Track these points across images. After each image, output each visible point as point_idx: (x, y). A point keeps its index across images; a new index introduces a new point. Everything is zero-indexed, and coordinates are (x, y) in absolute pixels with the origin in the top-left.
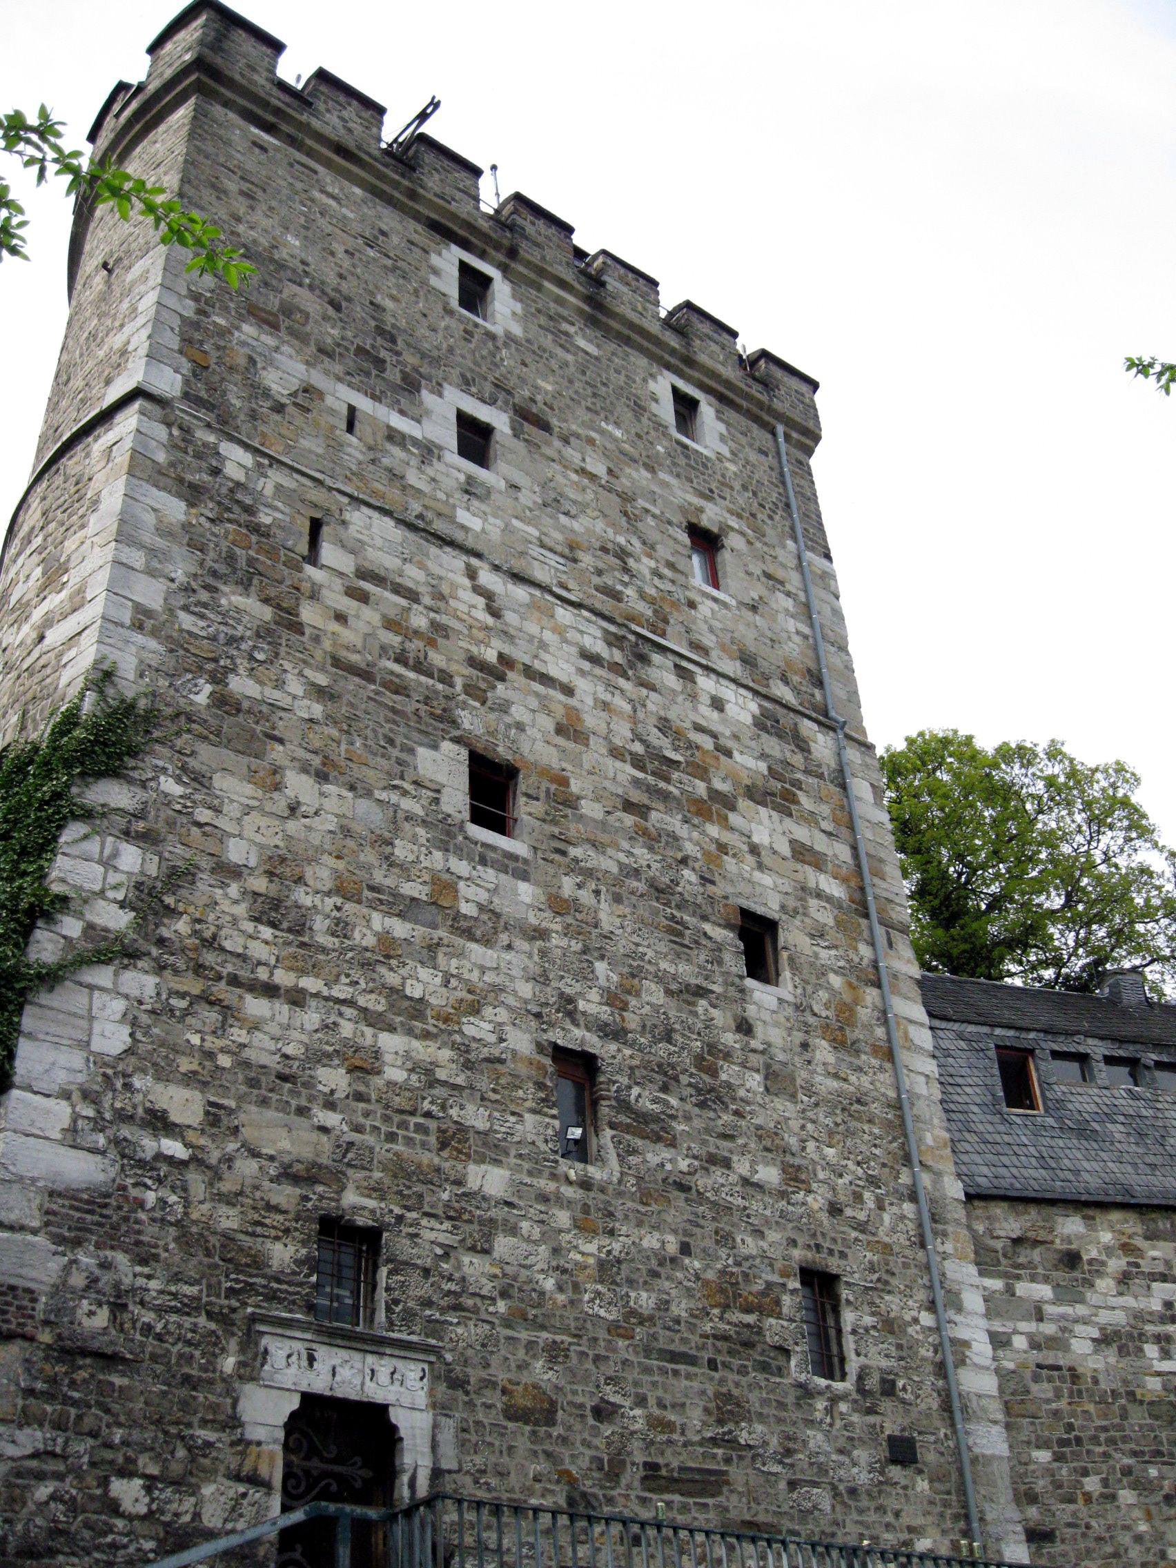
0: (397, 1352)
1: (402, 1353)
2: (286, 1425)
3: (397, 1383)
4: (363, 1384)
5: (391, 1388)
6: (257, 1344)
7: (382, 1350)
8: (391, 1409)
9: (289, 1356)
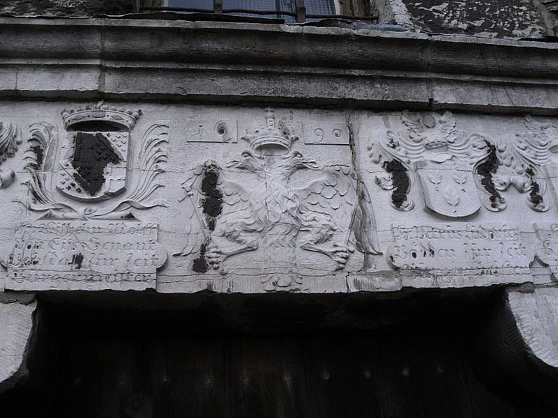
0: (480, 97)
1: (502, 99)
3: (517, 202)
4: (361, 224)
5: (490, 220)
7: (418, 94)
8: (514, 300)
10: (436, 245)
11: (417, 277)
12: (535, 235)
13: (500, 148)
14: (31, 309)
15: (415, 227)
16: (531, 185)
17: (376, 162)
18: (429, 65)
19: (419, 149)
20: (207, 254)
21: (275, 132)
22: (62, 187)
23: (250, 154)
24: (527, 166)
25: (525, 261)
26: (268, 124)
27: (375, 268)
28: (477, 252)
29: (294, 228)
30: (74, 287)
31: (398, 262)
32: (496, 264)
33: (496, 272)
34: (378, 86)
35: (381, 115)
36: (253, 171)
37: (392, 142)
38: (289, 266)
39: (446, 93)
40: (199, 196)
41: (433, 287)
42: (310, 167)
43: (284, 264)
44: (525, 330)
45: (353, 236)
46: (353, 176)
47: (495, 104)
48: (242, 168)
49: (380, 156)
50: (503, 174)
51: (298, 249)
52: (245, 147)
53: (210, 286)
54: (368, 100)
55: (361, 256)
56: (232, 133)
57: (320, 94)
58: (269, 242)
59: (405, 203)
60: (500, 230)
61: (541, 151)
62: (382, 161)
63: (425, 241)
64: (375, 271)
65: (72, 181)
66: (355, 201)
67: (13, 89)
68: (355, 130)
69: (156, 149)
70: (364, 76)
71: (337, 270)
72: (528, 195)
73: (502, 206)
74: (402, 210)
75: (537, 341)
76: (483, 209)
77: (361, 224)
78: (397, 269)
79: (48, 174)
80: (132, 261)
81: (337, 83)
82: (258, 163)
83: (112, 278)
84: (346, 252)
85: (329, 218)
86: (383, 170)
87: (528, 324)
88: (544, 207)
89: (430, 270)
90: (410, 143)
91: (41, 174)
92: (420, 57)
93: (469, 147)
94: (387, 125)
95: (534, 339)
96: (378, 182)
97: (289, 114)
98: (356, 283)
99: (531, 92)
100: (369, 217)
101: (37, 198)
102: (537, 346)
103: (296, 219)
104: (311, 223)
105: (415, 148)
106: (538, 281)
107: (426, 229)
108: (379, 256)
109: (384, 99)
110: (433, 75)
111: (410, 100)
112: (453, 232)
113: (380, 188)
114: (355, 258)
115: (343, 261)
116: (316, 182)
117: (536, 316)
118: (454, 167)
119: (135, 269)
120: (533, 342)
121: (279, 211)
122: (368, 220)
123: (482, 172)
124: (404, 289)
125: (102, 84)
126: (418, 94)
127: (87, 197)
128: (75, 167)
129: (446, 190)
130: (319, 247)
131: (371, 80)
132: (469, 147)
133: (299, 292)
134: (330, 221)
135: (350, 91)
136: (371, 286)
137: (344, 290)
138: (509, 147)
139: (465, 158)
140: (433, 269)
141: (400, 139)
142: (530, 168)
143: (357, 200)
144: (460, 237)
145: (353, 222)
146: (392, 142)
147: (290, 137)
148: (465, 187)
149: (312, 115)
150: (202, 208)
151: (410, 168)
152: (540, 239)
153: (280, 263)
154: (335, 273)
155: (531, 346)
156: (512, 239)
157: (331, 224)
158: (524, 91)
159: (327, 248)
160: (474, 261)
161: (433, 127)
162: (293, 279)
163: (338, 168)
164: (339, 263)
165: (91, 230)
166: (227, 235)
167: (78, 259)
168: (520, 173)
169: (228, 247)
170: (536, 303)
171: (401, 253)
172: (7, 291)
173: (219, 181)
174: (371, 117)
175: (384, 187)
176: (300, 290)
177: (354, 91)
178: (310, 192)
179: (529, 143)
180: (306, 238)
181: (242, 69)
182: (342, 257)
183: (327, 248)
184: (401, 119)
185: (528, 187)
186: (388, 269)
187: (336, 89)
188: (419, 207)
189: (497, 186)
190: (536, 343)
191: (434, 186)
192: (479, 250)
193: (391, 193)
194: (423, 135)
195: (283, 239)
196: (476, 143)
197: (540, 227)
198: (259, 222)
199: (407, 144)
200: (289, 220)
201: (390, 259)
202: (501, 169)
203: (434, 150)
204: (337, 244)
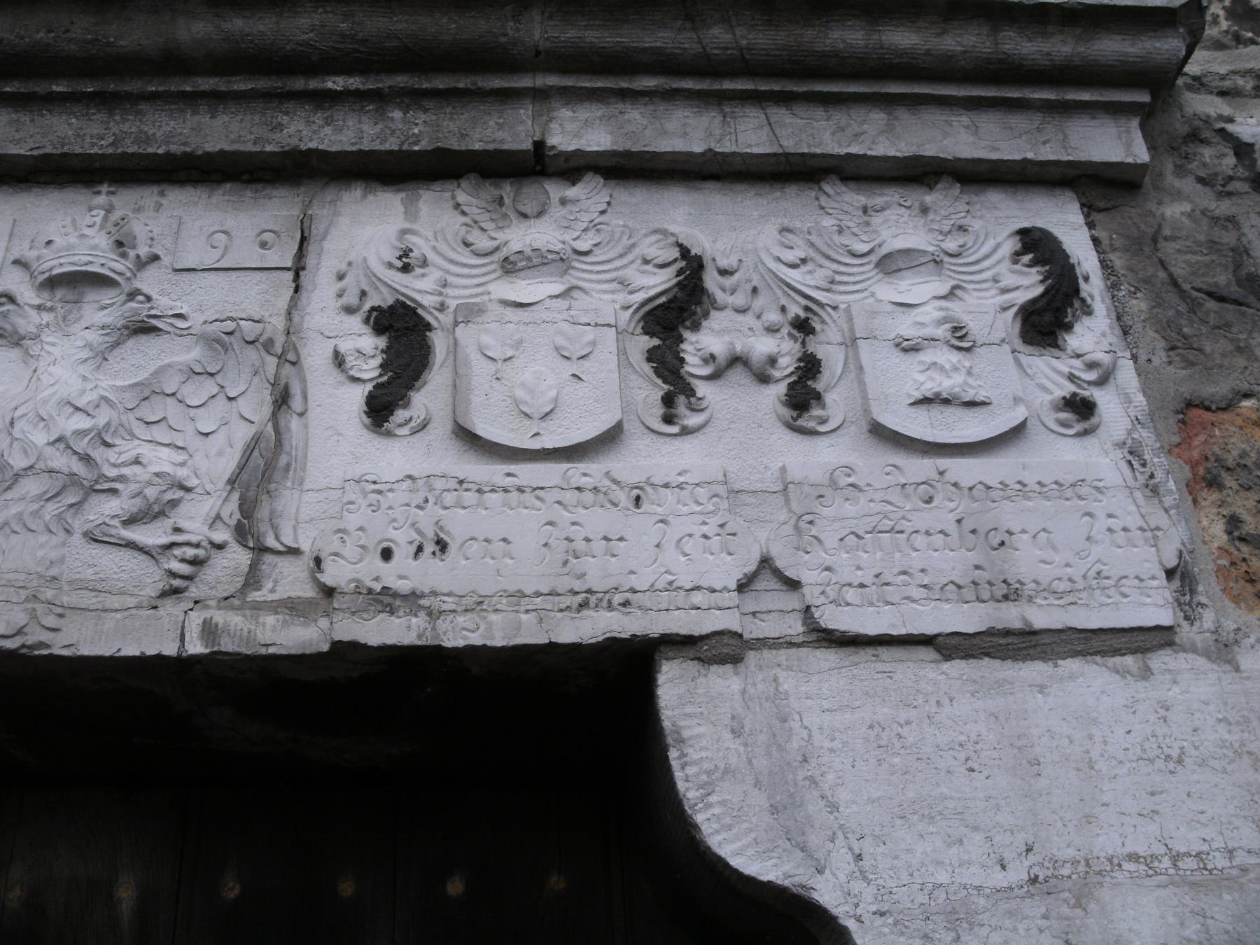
10: (459, 525)
11: (382, 616)
12: (780, 499)
13: (723, 263)
15: (410, 477)
16: (800, 360)
17: (349, 310)
18: (538, 53)
19: (483, 275)
21: (96, 241)
24: (795, 310)
25: (726, 572)
27: (272, 591)
28: (580, 545)
29: (73, 484)
32: (635, 582)
33: (626, 604)
34: (397, 114)
35: (399, 191)
37: (406, 253)
38: (35, 583)
39: (587, 123)
41: (420, 643)
42: (168, 328)
43: (22, 576)
44: (691, 770)
45: (232, 507)
47: (727, 147)
49: (363, 294)
50: (721, 332)
51: (77, 539)
54: (360, 151)
55: (239, 557)
57: (233, 142)
59: (400, 415)
60: (666, 486)
61: (855, 270)
62: (367, 307)
63: (426, 520)
64: (271, 597)
68: (317, 230)
70: (357, 90)
71: (164, 594)
73: (693, 420)
74: (389, 434)
75: (722, 803)
81: (287, 113)
84: (197, 546)
85: (181, 457)
86: (366, 330)
87: (704, 754)
88: (823, 421)
89: (422, 596)
90: (465, 261)
92: (510, 32)
93: (632, 262)
94: (411, 215)
95: (713, 799)
96: (339, 360)
97: (155, 198)
98: (209, 630)
99: (839, 116)
100: (289, 454)
102: (718, 818)
103: (86, 459)
104: (125, 471)
105: (475, 272)
106: (755, 629)
107: (439, 484)
108: (291, 558)
109: (405, 147)
110: (553, 80)
111: (477, 146)
112: (521, 490)
113: (341, 377)
114: (225, 563)
115: (185, 569)
116: (169, 365)
117: (733, 731)
118: (565, 315)
120: (709, 806)
121: (40, 438)
122: (283, 460)
123: (658, 328)
124: (338, 646)
129: (528, 376)
131: (379, 99)
132: (632, 262)
133: (45, 652)
134: (182, 464)
135: (315, 132)
136: (249, 638)
137: (170, 650)
138: (748, 262)
139: (613, 292)
140: (434, 593)
141: (434, 248)
142: (802, 315)
143: (267, 410)
144: (538, 503)
145: (242, 467)
146: (406, 253)
147: (132, 253)
148: (582, 368)
149: (214, 200)
152: (790, 511)
153: (12, 576)
154: (159, 602)
155: (699, 818)
156: (698, 508)
157: (182, 473)
158: (820, 112)
160: (566, 570)
161: (539, 214)
162: (33, 616)
163: (230, 326)
164: (173, 574)
168: (772, 330)
170: (744, 692)
171: (350, 551)
174: (371, 198)
175: (352, 373)
176: (48, 646)
177: (328, 130)
178: (148, 391)
179: (818, 250)
180: (108, 508)
181: (39, 87)
182: (183, 560)
184: (453, 197)
185: (787, 364)
186: (309, 592)
188: (441, 428)
189: (693, 365)
190: (717, 810)
191: (491, 367)
192: (588, 540)
193: (369, 387)
194: (501, 236)
195: (36, 514)
196: (652, 252)
197: (795, 474)
199: (452, 261)
200: (61, 461)
201: (312, 564)
202: (716, 320)
203: (522, 274)
204: (183, 524)
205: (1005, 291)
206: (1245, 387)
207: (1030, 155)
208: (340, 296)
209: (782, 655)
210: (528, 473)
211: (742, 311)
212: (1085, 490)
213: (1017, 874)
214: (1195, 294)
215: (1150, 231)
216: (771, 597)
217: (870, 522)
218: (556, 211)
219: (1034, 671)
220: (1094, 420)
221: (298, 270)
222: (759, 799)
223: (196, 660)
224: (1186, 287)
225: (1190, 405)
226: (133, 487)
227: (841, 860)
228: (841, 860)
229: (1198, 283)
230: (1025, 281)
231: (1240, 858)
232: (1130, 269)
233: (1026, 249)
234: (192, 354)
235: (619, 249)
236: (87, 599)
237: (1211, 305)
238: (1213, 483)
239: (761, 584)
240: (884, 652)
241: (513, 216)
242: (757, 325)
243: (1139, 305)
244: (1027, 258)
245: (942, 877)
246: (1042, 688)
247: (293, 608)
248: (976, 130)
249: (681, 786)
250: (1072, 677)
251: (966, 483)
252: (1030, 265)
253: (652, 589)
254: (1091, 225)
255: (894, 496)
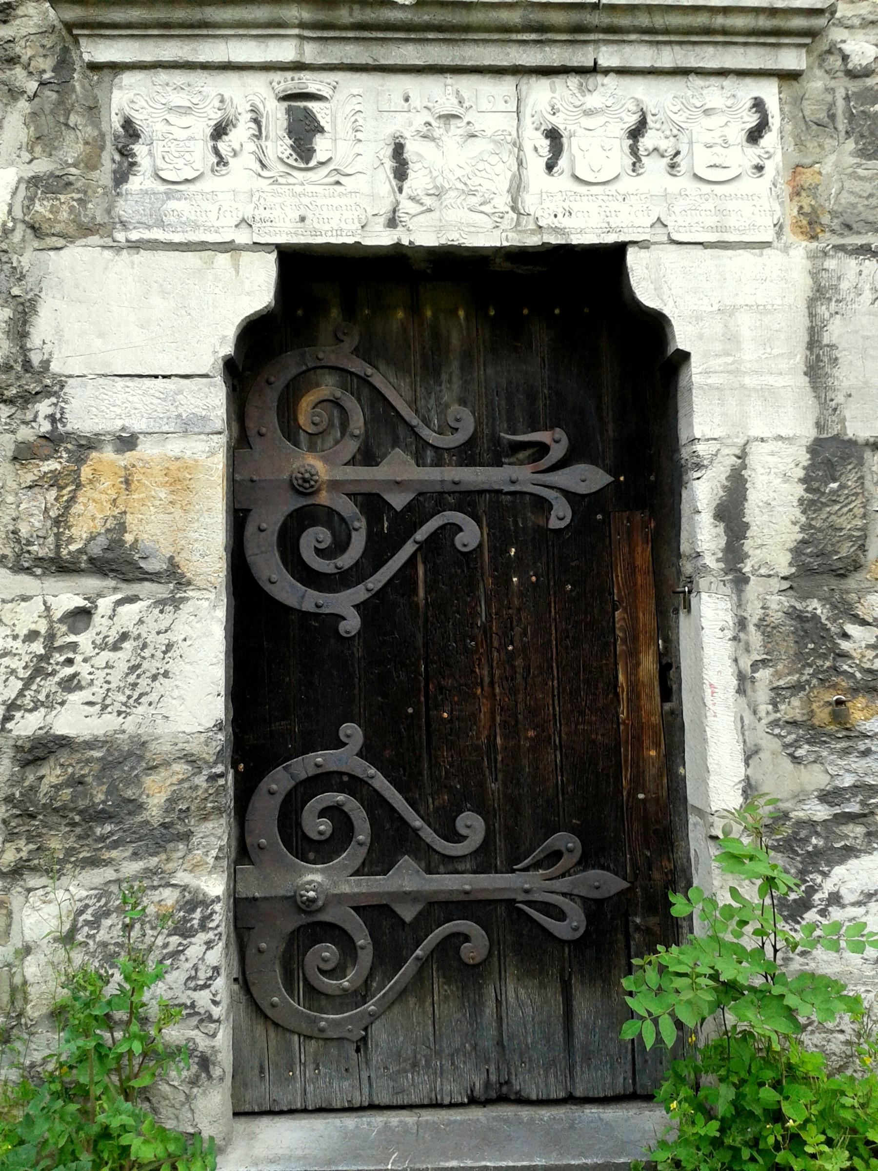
2: (230, 366)
4: (517, 188)
5: (628, 183)
6: (93, 110)
7: (583, 57)
9: (220, 131)
10: (575, 207)
13: (653, 112)
14: (274, 255)
17: (537, 129)
20: (397, 214)
22: (280, 155)
23: (430, 125)
26: (447, 92)
28: (608, 214)
30: (303, 240)
31: (540, 224)
36: (433, 139)
39: (612, 54)
40: (389, 164)
45: (510, 199)
46: (514, 144)
48: (425, 137)
52: (427, 117)
53: (399, 239)
55: (515, 216)
56: (416, 101)
58: (444, 204)
59: (555, 169)
62: (543, 128)
65: (290, 151)
66: (515, 168)
67: (227, 60)
69: (353, 119)
72: (666, 161)
73: (641, 171)
76: (623, 174)
77: (517, 188)
78: (540, 227)
79: (269, 143)
80: (343, 220)
82: (437, 133)
83: (330, 233)
86: (543, 137)
88: (679, 172)
91: (263, 143)
94: (553, 90)
96: (536, 149)
101: (263, 166)
103: (465, 184)
107: (569, 194)
110: (601, 36)
115: (499, 220)
119: (343, 226)
122: (523, 185)
125: (302, 54)
126: (583, 57)
127: (303, 166)
128: (290, 138)
130: (483, 208)
137: (498, 245)
143: (516, 167)
147: (464, 105)
148: (609, 153)
150: (392, 176)
151: (565, 134)
159: (487, 208)
163: (503, 137)
165: (310, 195)
166: (412, 198)
167: (303, 219)
169: (413, 208)
171: (546, 215)
172: (255, 243)
173: (406, 150)
177: (525, 55)
180: (474, 201)
183: (487, 208)
186: (534, 227)
187: (508, 54)
189: (642, 152)
193: (546, 159)
198: (436, 187)
200: (461, 186)
205: (744, 123)
206: (818, 160)
207: (762, 67)
208: (533, 123)
209: (661, 246)
210: (595, 189)
211: (658, 130)
212: (754, 197)
213: (716, 308)
214: (810, 123)
215: (801, 95)
216: (659, 229)
217: (689, 207)
218: (601, 89)
219: (729, 253)
220: (763, 172)
221: (518, 113)
222: (652, 286)
223: (505, 247)
224: (807, 119)
225: (797, 166)
226: (481, 194)
227: (671, 303)
228: (671, 303)
229: (812, 119)
230: (751, 119)
231: (775, 307)
232: (790, 112)
233: (754, 106)
234: (491, 147)
235: (620, 105)
236: (473, 229)
237: (815, 127)
238: (798, 194)
239: (656, 225)
240: (689, 246)
241: (586, 91)
242: (662, 135)
243: (789, 127)
244: (754, 110)
245: (696, 308)
246: (731, 258)
247: (533, 232)
248: (745, 55)
249: (632, 282)
250: (740, 255)
251: (719, 195)
252: (756, 112)
253: (627, 227)
254: (780, 93)
255: (698, 198)
